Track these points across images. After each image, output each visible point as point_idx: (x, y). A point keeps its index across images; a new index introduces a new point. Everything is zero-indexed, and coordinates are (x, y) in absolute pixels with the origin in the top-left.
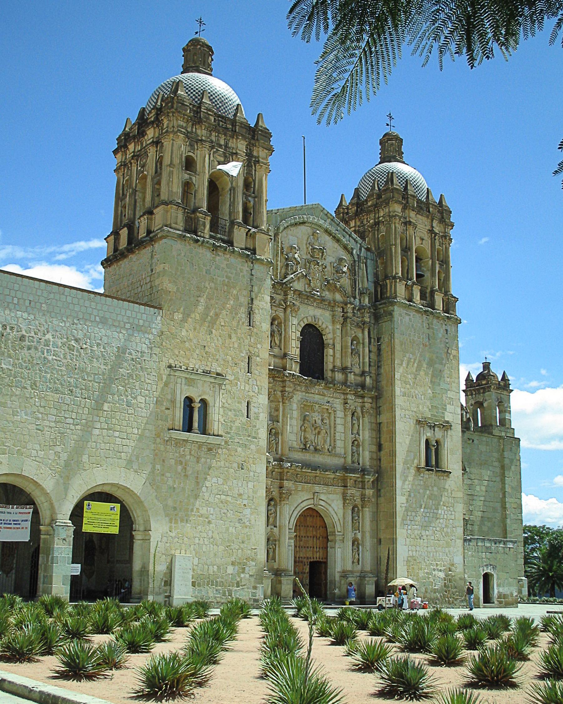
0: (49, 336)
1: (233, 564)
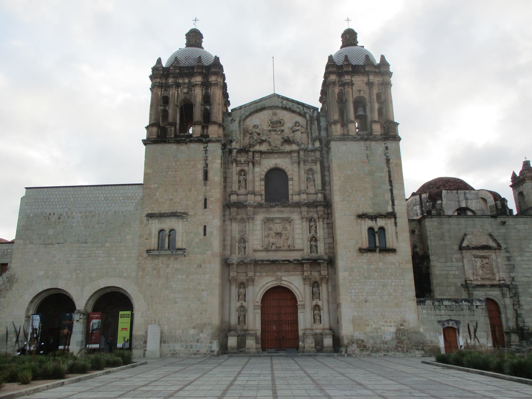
1: (194, 328)
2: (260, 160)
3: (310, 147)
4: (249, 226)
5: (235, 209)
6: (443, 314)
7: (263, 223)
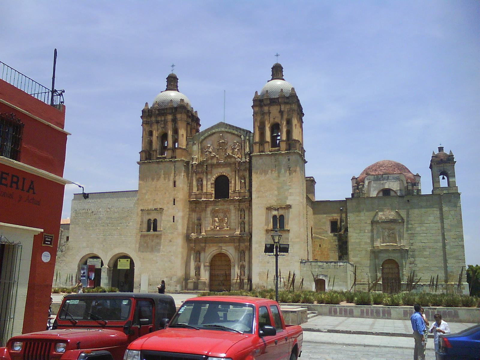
0: (100, 210)
1: (167, 277)
2: (211, 170)
3: (244, 160)
4: (203, 215)
5: (194, 204)
6: (317, 271)
7: (212, 212)
